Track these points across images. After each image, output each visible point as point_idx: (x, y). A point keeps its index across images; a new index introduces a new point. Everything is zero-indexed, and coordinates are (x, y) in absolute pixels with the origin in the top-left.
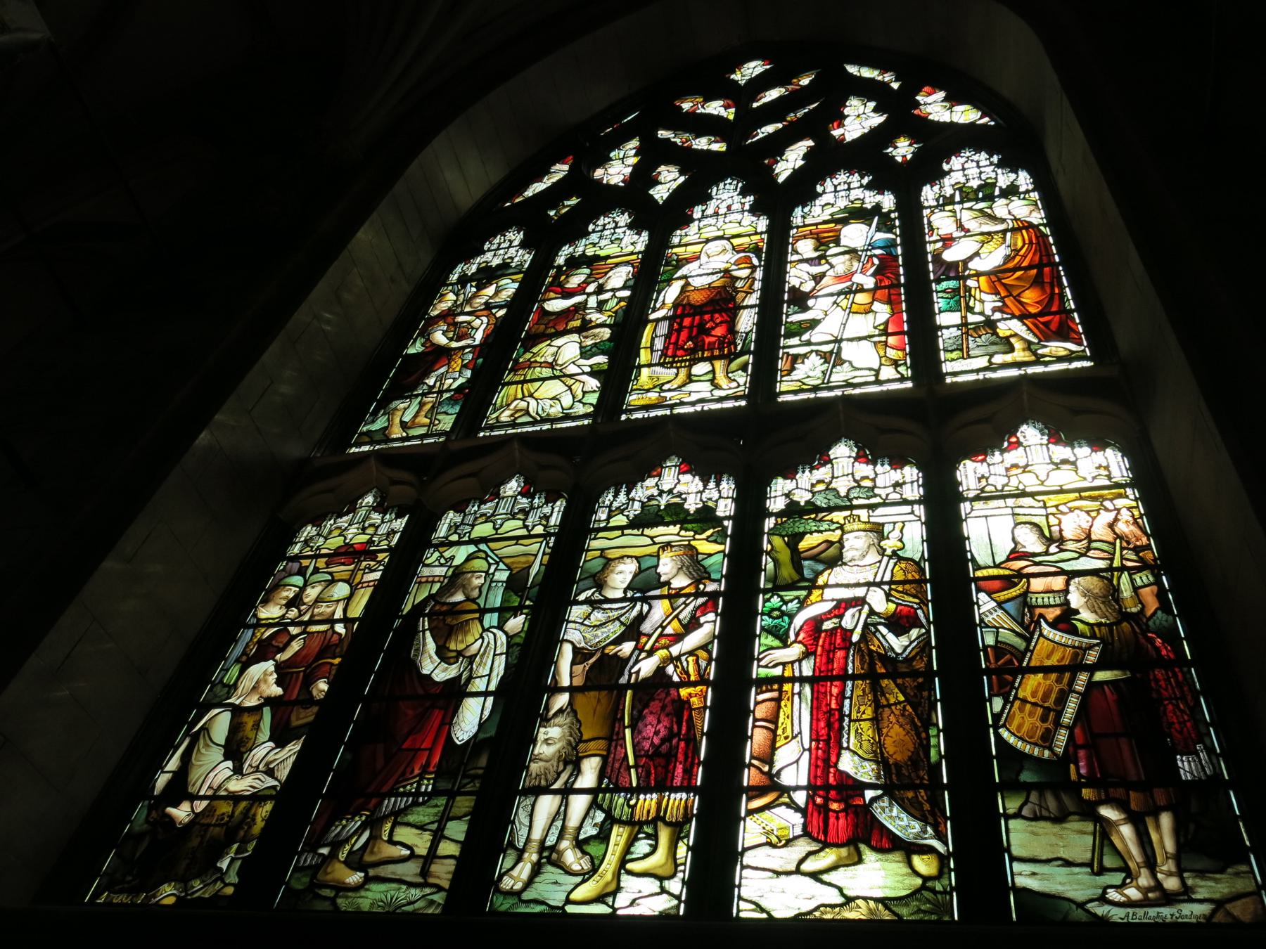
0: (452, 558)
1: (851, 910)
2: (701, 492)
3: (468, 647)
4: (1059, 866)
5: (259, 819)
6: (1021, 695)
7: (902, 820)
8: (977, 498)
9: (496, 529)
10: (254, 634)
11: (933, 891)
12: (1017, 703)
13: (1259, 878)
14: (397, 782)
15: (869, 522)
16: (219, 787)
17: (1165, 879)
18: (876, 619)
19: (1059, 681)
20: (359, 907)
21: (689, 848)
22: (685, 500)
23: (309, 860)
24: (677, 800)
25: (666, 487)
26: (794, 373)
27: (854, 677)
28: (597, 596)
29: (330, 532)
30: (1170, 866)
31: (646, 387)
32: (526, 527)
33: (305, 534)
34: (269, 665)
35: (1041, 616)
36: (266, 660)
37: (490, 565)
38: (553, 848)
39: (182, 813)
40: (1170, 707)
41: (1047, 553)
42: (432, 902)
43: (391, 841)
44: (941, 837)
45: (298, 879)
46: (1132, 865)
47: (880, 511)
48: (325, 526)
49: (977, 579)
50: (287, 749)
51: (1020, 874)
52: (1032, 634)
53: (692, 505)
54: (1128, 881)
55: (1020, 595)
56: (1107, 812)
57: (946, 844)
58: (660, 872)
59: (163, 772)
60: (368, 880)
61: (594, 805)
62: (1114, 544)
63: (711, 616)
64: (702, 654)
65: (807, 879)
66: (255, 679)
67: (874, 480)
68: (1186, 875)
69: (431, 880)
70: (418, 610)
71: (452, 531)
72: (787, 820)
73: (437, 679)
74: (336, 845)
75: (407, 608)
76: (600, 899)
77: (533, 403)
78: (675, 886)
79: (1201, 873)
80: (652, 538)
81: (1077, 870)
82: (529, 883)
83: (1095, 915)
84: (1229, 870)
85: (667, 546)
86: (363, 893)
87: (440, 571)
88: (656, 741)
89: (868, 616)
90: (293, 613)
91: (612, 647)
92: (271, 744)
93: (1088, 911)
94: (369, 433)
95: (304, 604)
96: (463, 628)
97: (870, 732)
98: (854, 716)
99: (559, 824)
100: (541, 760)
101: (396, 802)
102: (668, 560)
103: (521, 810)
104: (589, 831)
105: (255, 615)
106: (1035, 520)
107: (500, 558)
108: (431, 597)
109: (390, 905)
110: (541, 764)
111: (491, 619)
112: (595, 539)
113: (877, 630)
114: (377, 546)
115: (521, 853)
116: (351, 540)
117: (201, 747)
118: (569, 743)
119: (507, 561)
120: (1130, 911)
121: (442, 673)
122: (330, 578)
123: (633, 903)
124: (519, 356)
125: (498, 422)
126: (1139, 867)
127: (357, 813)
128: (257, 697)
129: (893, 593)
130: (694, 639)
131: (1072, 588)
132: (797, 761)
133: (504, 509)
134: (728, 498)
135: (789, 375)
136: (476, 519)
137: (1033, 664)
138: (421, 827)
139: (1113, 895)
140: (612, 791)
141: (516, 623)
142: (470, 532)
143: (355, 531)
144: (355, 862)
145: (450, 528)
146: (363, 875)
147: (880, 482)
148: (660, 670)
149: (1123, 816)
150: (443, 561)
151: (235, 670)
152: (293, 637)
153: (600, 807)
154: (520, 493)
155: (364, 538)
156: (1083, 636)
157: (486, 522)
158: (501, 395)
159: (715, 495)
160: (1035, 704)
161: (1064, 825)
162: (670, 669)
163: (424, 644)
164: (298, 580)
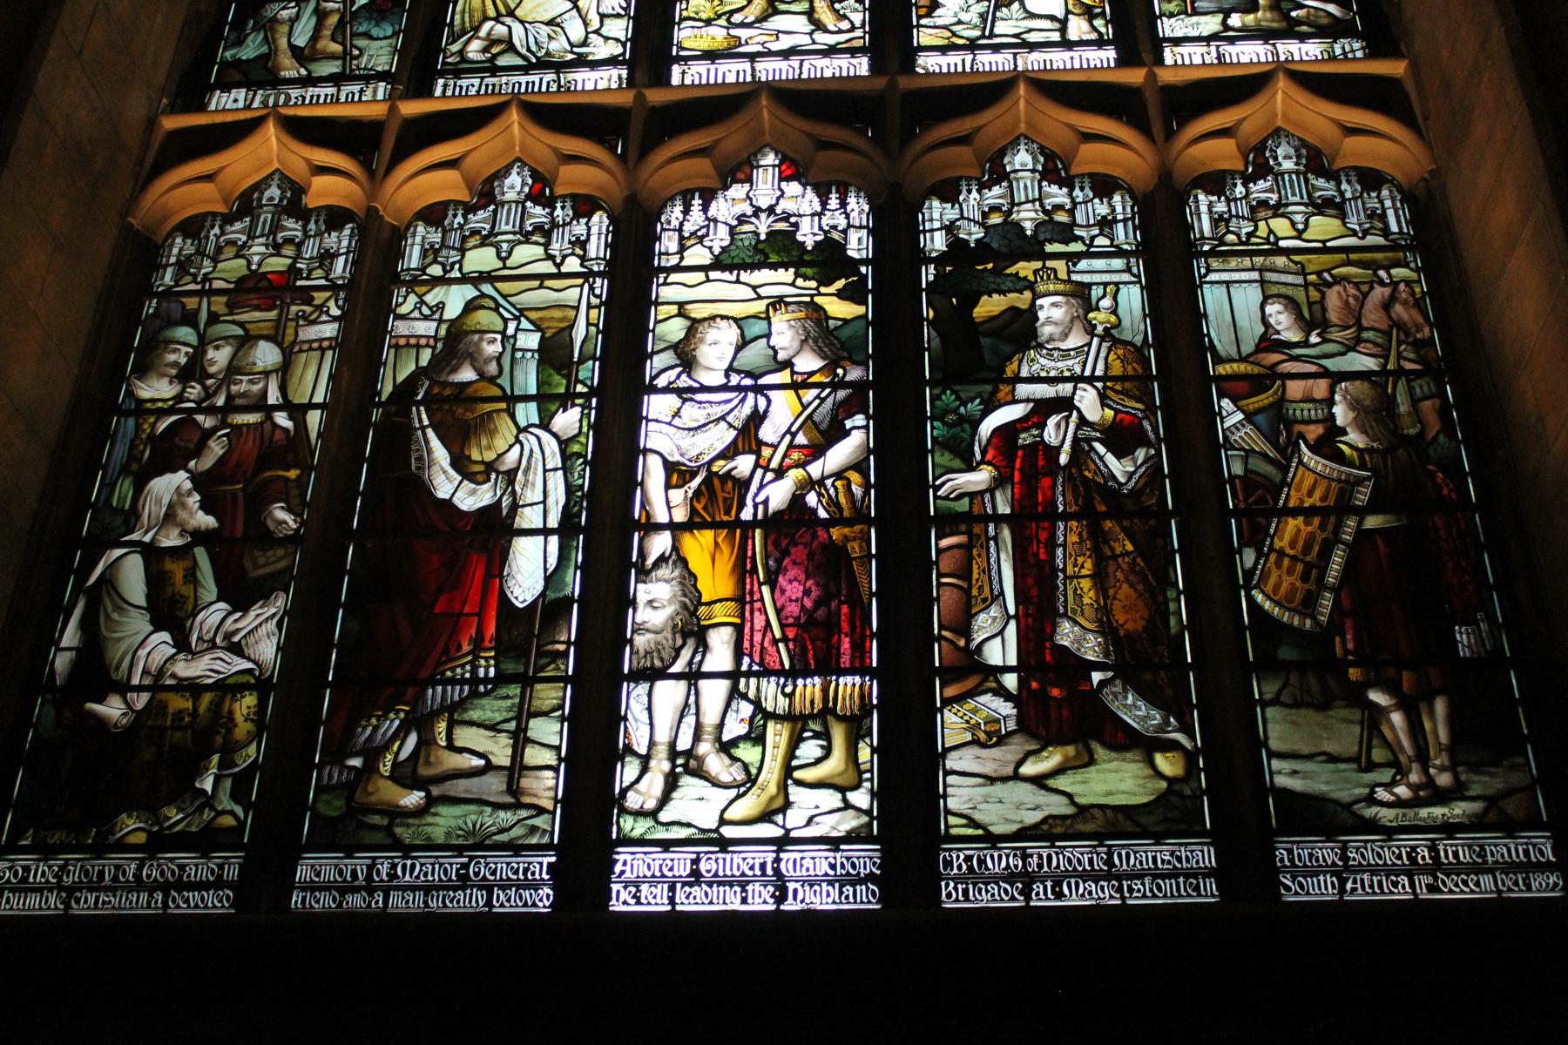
0: (441, 306)
1: (1085, 821)
2: (820, 215)
3: (500, 456)
4: (1322, 762)
5: (239, 718)
6: (1278, 544)
7: (1140, 709)
8: (1213, 253)
9: (504, 260)
10: (138, 427)
11: (1181, 795)
12: (1273, 557)
13: (1534, 771)
14: (439, 663)
15: (1069, 281)
16: (161, 671)
17: (1437, 775)
18: (1087, 432)
19: (1322, 527)
20: (429, 838)
21: (873, 751)
22: (796, 225)
24: (848, 684)
25: (764, 203)
26: (938, 12)
27: (1066, 517)
28: (685, 381)
29: (219, 250)
30: (1441, 760)
31: (704, 16)
32: (550, 257)
33: (175, 251)
34: (180, 478)
35: (1301, 436)
36: (174, 470)
37: (505, 321)
38: (689, 754)
39: (113, 709)
40: (1450, 564)
41: (1305, 344)
42: (533, 830)
43: (451, 747)
44: (1187, 729)
45: (328, 803)
46: (1402, 759)
47: (1083, 264)
48: (207, 237)
49: (1219, 379)
50: (252, 614)
51: (1280, 773)
52: (1289, 461)
53: (808, 235)
54: (1398, 777)
55: (1272, 405)
56: (1377, 697)
57: (1192, 737)
58: (839, 781)
59: (59, 649)
60: (431, 801)
61: (735, 694)
62: (1388, 334)
63: (859, 420)
64: (854, 477)
65: (1028, 787)
66: (166, 501)
67: (1071, 212)
68: (1459, 769)
69: (526, 800)
70: (405, 392)
71: (429, 259)
73: (464, 507)
74: (373, 754)
75: (387, 389)
76: (766, 817)
77: (518, 29)
78: (860, 798)
79: (1476, 768)
80: (754, 288)
81: (1342, 766)
83: (1362, 817)
84: (1505, 763)
85: (778, 302)
86: (430, 819)
87: (426, 328)
88: (808, 603)
89: (1078, 428)
90: (195, 391)
91: (721, 463)
92: (222, 605)
93: (1354, 814)
94: (237, 63)
95: (210, 376)
96: (484, 425)
97: (1092, 594)
98: (1070, 571)
99: (690, 720)
100: (648, 630)
101: (444, 691)
102: (785, 325)
103: (632, 702)
104: (734, 729)
105: (130, 393)
106: (1289, 291)
107: (520, 310)
108: (419, 373)
109: (473, 833)
110: (649, 636)
111: (527, 413)
112: (665, 284)
113: (1093, 449)
114: (308, 278)
115: (645, 761)
116: (260, 265)
117: (110, 609)
118: (684, 606)
119: (534, 315)
120: (1400, 811)
121: (472, 498)
122: (240, 332)
123: (810, 821)
125: (464, 60)
126: (1411, 762)
127: (388, 708)
128: (177, 531)
129: (1110, 394)
130: (840, 454)
131: (1337, 397)
132: (1001, 633)
133: (507, 223)
134: (861, 227)
135: (929, 15)
136: (464, 239)
137: (1291, 504)
138: (493, 727)
139: (1381, 794)
140: (758, 675)
141: (568, 420)
142: (460, 262)
143: (262, 249)
144: (406, 776)
145: (424, 254)
146: (423, 794)
147: (1080, 218)
148: (797, 500)
149: (1393, 702)
150: (426, 311)
151: (125, 488)
152: (210, 433)
153: (745, 697)
154: (529, 197)
155: (278, 264)
156: (1351, 465)
157: (482, 245)
158: (459, 8)
159: (842, 222)
160: (1294, 558)
161: (1331, 713)
162: (812, 499)
163: (429, 451)
164: (185, 333)
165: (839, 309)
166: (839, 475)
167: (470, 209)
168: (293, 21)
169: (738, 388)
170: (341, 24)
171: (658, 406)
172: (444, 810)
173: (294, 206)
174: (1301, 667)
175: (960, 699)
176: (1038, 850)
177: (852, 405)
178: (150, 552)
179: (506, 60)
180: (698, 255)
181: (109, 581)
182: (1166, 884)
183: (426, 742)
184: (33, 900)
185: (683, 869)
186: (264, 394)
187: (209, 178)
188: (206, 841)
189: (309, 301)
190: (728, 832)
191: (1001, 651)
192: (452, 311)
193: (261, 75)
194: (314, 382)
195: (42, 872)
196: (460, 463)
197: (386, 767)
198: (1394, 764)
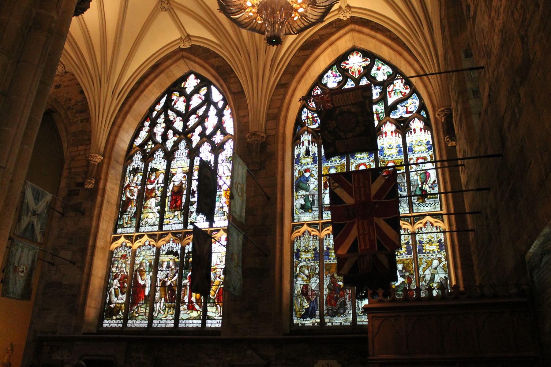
16: (116, 302)
23: (131, 313)
25: (171, 246)
38: (160, 311)
39: (112, 306)
44: (201, 309)
56: (218, 306)
60: (139, 315)
61: (164, 305)
63: (177, 274)
70: (136, 271)
72: (186, 307)
74: (134, 311)
75: (135, 270)
76: (165, 317)
78: (173, 316)
82: (157, 315)
85: (171, 259)
90: (118, 270)
96: (144, 275)
104: (164, 308)
111: (148, 273)
115: (156, 311)
124: (144, 204)
130: (175, 278)
138: (144, 308)
144: (137, 313)
148: (171, 283)
151: (112, 281)
152: (119, 275)
155: (125, 253)
159: (178, 249)
162: (172, 283)
164: (116, 262)
165: (177, 260)
166: (175, 281)
167: (143, 246)
168: (126, 218)
169: (167, 270)
170: (130, 219)
171: (159, 272)
172: (140, 316)
173: (126, 246)
174: (212, 303)
175: (182, 306)
176: (187, 321)
177: (176, 273)
178: (114, 289)
179: (147, 225)
180: (164, 253)
181: (111, 292)
182: (197, 325)
183: (138, 309)
184: (107, 325)
185: (158, 322)
186: (124, 271)
187: (117, 243)
188: (120, 319)
189: (128, 258)
190: (162, 319)
191: (186, 300)
192: (141, 260)
193: (122, 226)
194: (128, 270)
195: (107, 322)
196: (141, 279)
197: (135, 312)
198: (218, 313)
